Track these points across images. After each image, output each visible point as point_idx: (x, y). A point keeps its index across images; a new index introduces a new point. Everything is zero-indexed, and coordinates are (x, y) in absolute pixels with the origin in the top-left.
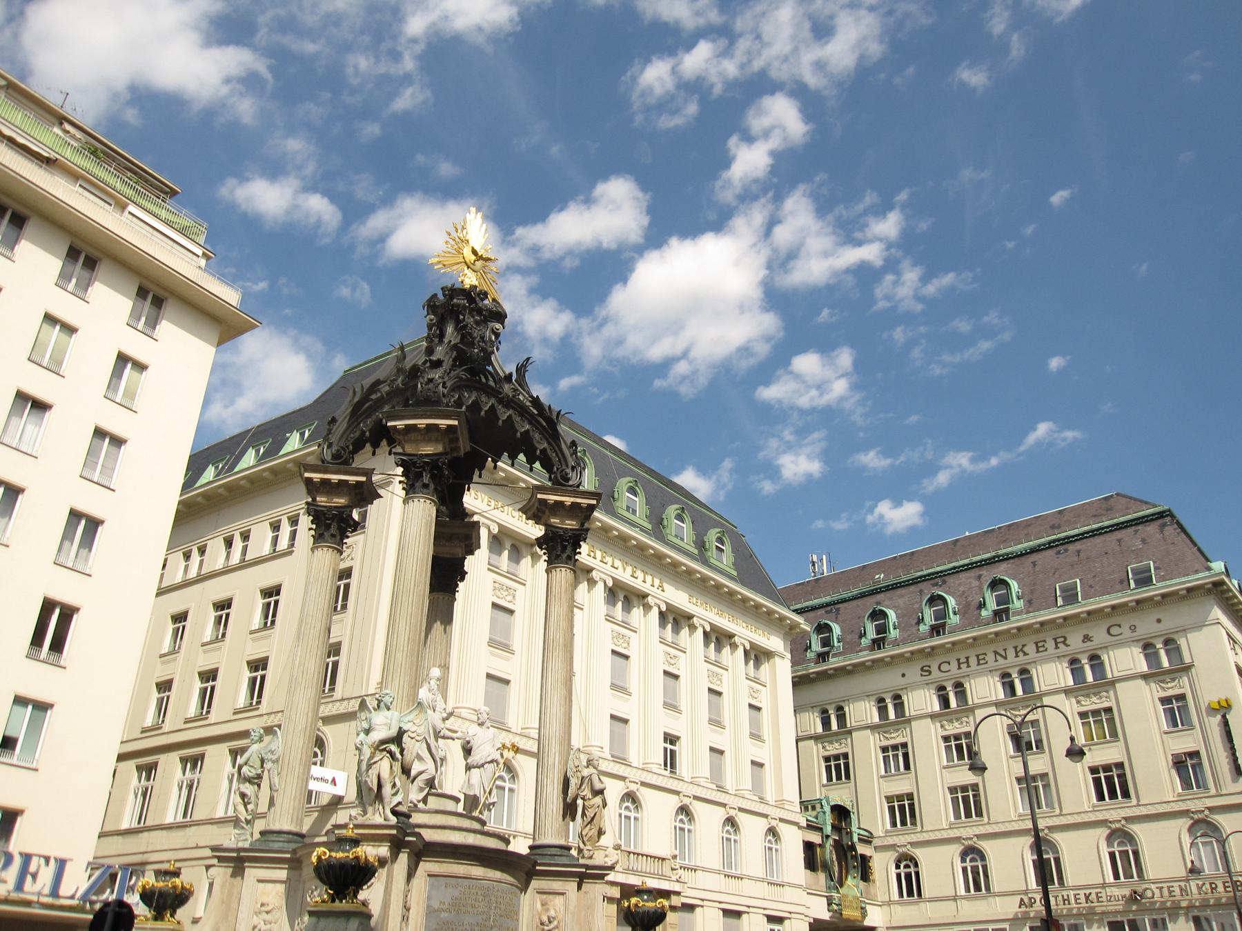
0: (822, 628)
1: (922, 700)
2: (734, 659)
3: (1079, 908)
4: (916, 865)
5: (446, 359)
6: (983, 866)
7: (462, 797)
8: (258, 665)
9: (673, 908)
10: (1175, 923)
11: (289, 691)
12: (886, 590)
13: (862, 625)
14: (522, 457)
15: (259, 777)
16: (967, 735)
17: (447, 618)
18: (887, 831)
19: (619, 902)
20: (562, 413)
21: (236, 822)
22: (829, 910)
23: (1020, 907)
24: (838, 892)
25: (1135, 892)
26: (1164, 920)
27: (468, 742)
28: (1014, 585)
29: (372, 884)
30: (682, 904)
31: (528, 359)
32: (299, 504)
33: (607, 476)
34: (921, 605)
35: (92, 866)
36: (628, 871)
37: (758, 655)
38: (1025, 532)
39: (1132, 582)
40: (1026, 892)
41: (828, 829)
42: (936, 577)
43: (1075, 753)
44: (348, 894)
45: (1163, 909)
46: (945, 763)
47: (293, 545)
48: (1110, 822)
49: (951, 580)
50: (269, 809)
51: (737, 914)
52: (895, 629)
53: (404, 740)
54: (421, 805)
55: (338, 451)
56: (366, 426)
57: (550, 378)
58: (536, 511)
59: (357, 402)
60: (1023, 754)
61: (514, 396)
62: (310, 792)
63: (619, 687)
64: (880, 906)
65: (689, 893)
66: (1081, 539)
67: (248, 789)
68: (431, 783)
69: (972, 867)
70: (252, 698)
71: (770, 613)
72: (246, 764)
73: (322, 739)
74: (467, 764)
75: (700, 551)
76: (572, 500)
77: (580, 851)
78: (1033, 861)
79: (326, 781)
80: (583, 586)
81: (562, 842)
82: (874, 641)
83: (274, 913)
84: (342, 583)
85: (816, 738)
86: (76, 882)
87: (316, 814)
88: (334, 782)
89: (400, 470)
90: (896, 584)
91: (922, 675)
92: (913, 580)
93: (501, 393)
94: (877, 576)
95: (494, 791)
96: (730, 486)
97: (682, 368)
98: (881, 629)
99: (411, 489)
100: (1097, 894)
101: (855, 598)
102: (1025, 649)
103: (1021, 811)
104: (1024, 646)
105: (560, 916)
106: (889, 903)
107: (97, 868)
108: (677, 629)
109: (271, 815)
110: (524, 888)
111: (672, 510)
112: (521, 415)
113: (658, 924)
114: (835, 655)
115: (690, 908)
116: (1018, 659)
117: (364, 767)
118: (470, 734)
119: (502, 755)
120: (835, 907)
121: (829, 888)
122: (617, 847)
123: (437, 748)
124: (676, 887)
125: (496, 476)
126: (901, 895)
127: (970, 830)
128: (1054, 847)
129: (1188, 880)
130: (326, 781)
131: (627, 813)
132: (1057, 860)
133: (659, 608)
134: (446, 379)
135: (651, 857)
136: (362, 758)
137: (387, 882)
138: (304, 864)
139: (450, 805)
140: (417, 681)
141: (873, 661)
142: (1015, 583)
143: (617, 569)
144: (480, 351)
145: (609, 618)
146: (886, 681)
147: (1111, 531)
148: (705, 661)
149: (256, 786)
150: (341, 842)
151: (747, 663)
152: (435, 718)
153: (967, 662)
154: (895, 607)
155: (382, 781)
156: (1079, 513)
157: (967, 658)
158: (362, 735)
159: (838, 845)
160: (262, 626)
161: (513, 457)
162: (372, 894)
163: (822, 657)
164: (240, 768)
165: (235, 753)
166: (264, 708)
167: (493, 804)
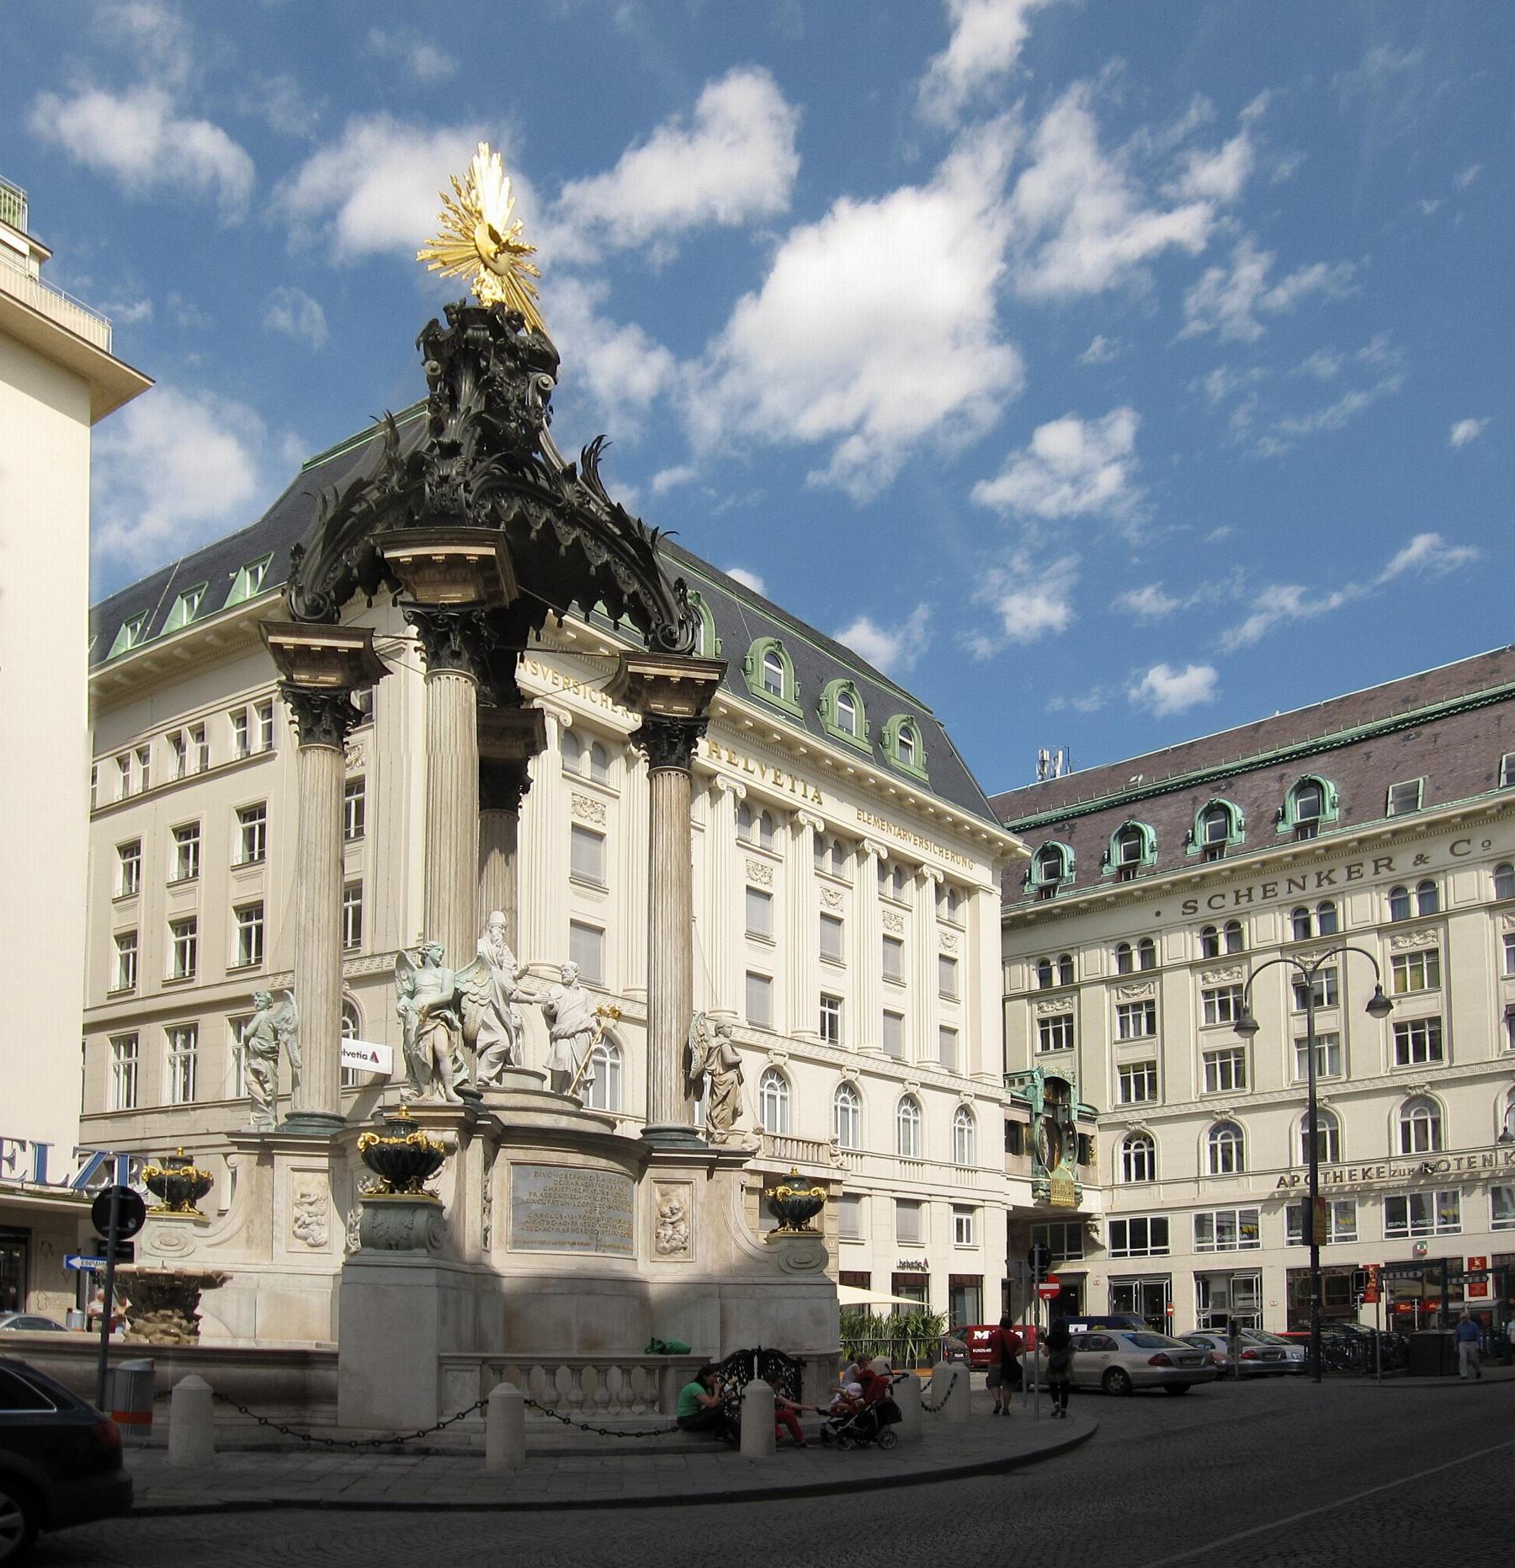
0: (1049, 854)
1: (1180, 945)
2: (921, 897)
3: (1353, 1185)
4: (1151, 1144)
5: (465, 442)
6: (1237, 1143)
7: (548, 1074)
8: (251, 911)
9: (832, 1198)
10: (1469, 1196)
11: (297, 944)
12: (1145, 798)
13: (1106, 847)
14: (600, 607)
15: (274, 1051)
16: (1237, 988)
17: (509, 846)
18: (1117, 1107)
19: (761, 1192)
20: (660, 532)
21: (252, 1103)
22: (1033, 1197)
23: (1278, 1187)
24: (1048, 1177)
25: (1427, 1165)
26: (1455, 1194)
27: (552, 1007)
28: (1331, 788)
29: (440, 1173)
30: (844, 1193)
31: (600, 438)
32: (270, 684)
33: (734, 634)
34: (1193, 818)
35: (80, 1152)
36: (771, 1158)
37: (954, 891)
38: (1364, 708)
39: (1504, 777)
40: (1288, 1171)
41: (1039, 1106)
42: (1219, 779)
43: (1379, 1005)
44: (410, 1184)
45: (1459, 1180)
46: (1203, 1024)
47: (270, 746)
48: (1410, 1088)
49: (1242, 783)
50: (293, 1090)
51: (916, 1203)
52: (1152, 851)
53: (463, 1004)
54: (494, 1084)
55: (314, 600)
56: (352, 558)
57: (637, 475)
58: (628, 690)
59: (332, 518)
60: (1309, 1011)
61: (581, 505)
62: (345, 1070)
63: (759, 937)
64: (1100, 1190)
65: (853, 1181)
66: (1444, 717)
67: (263, 1065)
68: (504, 1057)
69: (1223, 1144)
70: (249, 955)
71: (975, 832)
72: (254, 1035)
73: (351, 1006)
74: (552, 1034)
75: (876, 749)
76: (682, 673)
77: (709, 1135)
78: (1303, 1135)
79: (365, 1057)
80: (703, 800)
81: (685, 1125)
82: (1121, 869)
83: (318, 1203)
84: (352, 799)
85: (1030, 996)
86: (64, 1169)
87: (357, 1096)
88: (374, 1057)
89: (413, 630)
90: (1160, 789)
91: (1184, 913)
92: (1184, 783)
93: (560, 500)
94: (1133, 779)
95: (591, 1067)
96: (925, 649)
97: (854, 450)
98: (1134, 853)
99: (436, 658)
100: (1378, 1168)
101: (1099, 810)
102: (1332, 876)
103: (1297, 1078)
104: (1331, 871)
105: (686, 1208)
106: (1112, 1187)
107: (88, 1155)
108: (839, 857)
109: (296, 1097)
110: (638, 1177)
111: (834, 687)
112: (595, 537)
113: (813, 1215)
114: (1063, 889)
115: (855, 1198)
116: (1320, 889)
117: (412, 1038)
118: (553, 996)
119: (599, 1023)
120: (1042, 1193)
121: (1035, 1173)
122: (759, 1131)
123: (509, 1014)
124: (837, 1175)
125: (563, 639)
126: (1128, 1177)
127: (1225, 1102)
128: (1332, 1119)
129: (1495, 1150)
130: (365, 1057)
131: (772, 1092)
132: (1334, 1134)
133: (814, 827)
134: (469, 476)
135: (803, 1142)
136: (408, 1027)
137: (459, 1170)
138: (348, 1152)
139: (533, 1084)
140: (474, 928)
141: (1117, 896)
142: (1331, 786)
143: (752, 772)
144: (520, 425)
145: (742, 843)
146: (1131, 922)
147: (1490, 704)
148: (880, 899)
149: (272, 1062)
150: (393, 1125)
151: (938, 901)
152: (504, 977)
153: (1250, 895)
154: (1155, 821)
155: (439, 1055)
156: (1446, 680)
157: (1250, 890)
158: (405, 1000)
159: (1051, 1125)
160: (247, 860)
161: (587, 607)
162: (441, 1184)
163: (1046, 892)
164: (247, 1040)
165: (238, 1023)
166: (267, 966)
167: (591, 1081)
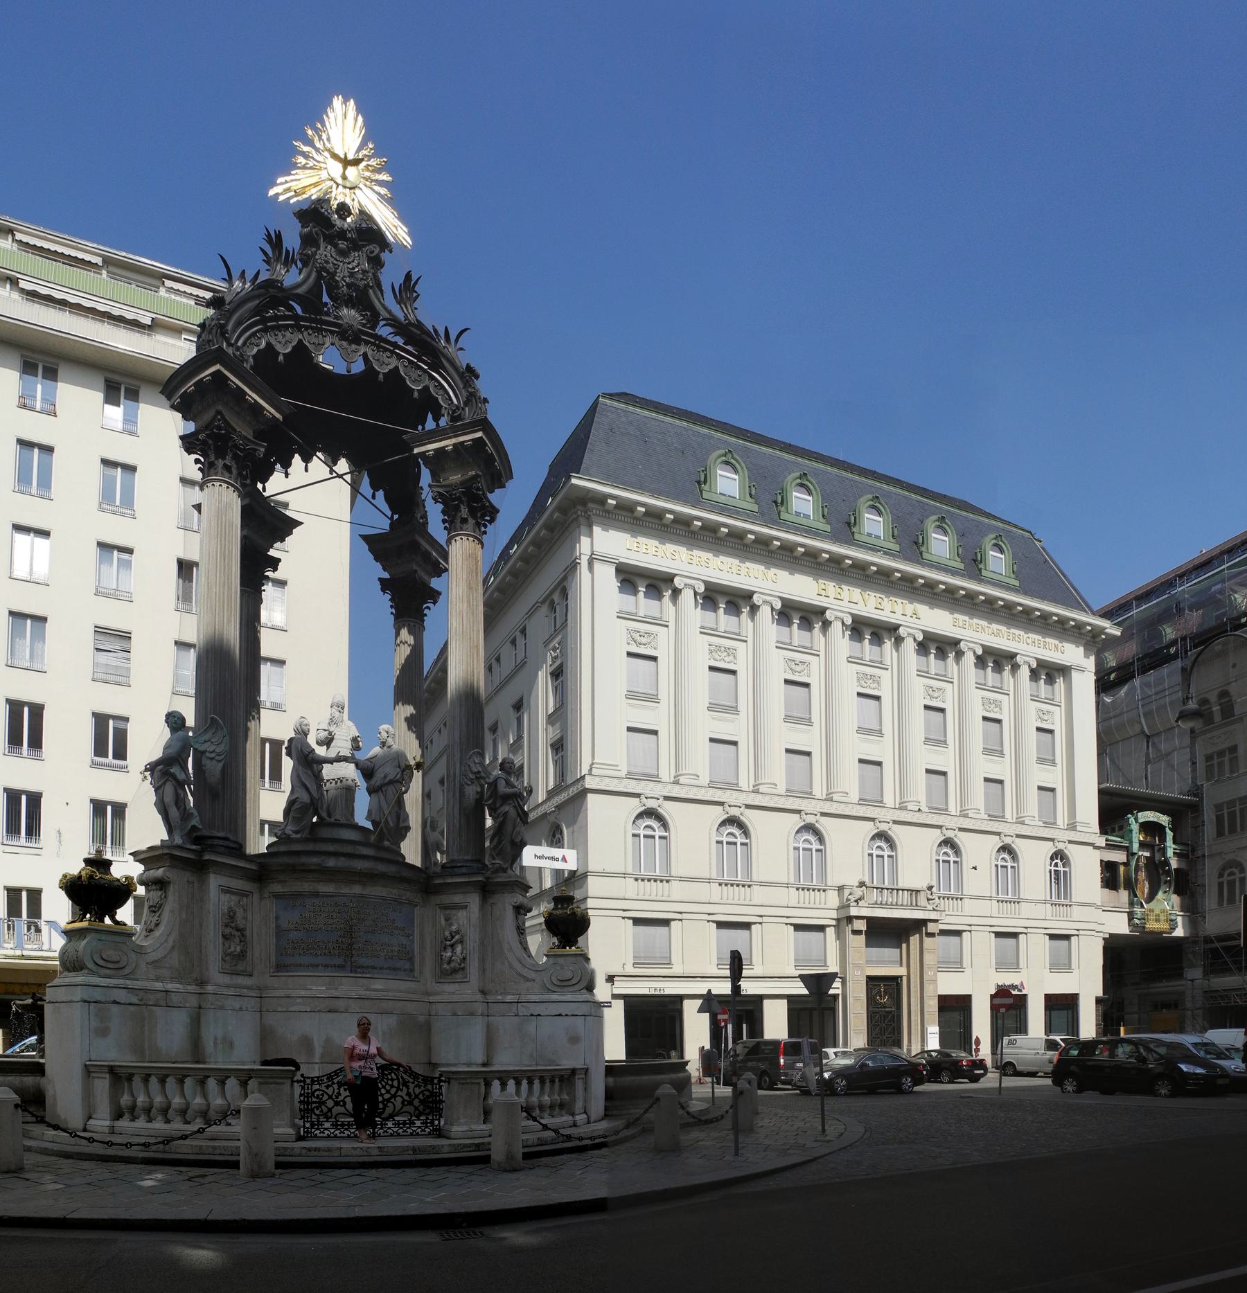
30: (940, 930)
120: (1137, 921)
124: (933, 916)
